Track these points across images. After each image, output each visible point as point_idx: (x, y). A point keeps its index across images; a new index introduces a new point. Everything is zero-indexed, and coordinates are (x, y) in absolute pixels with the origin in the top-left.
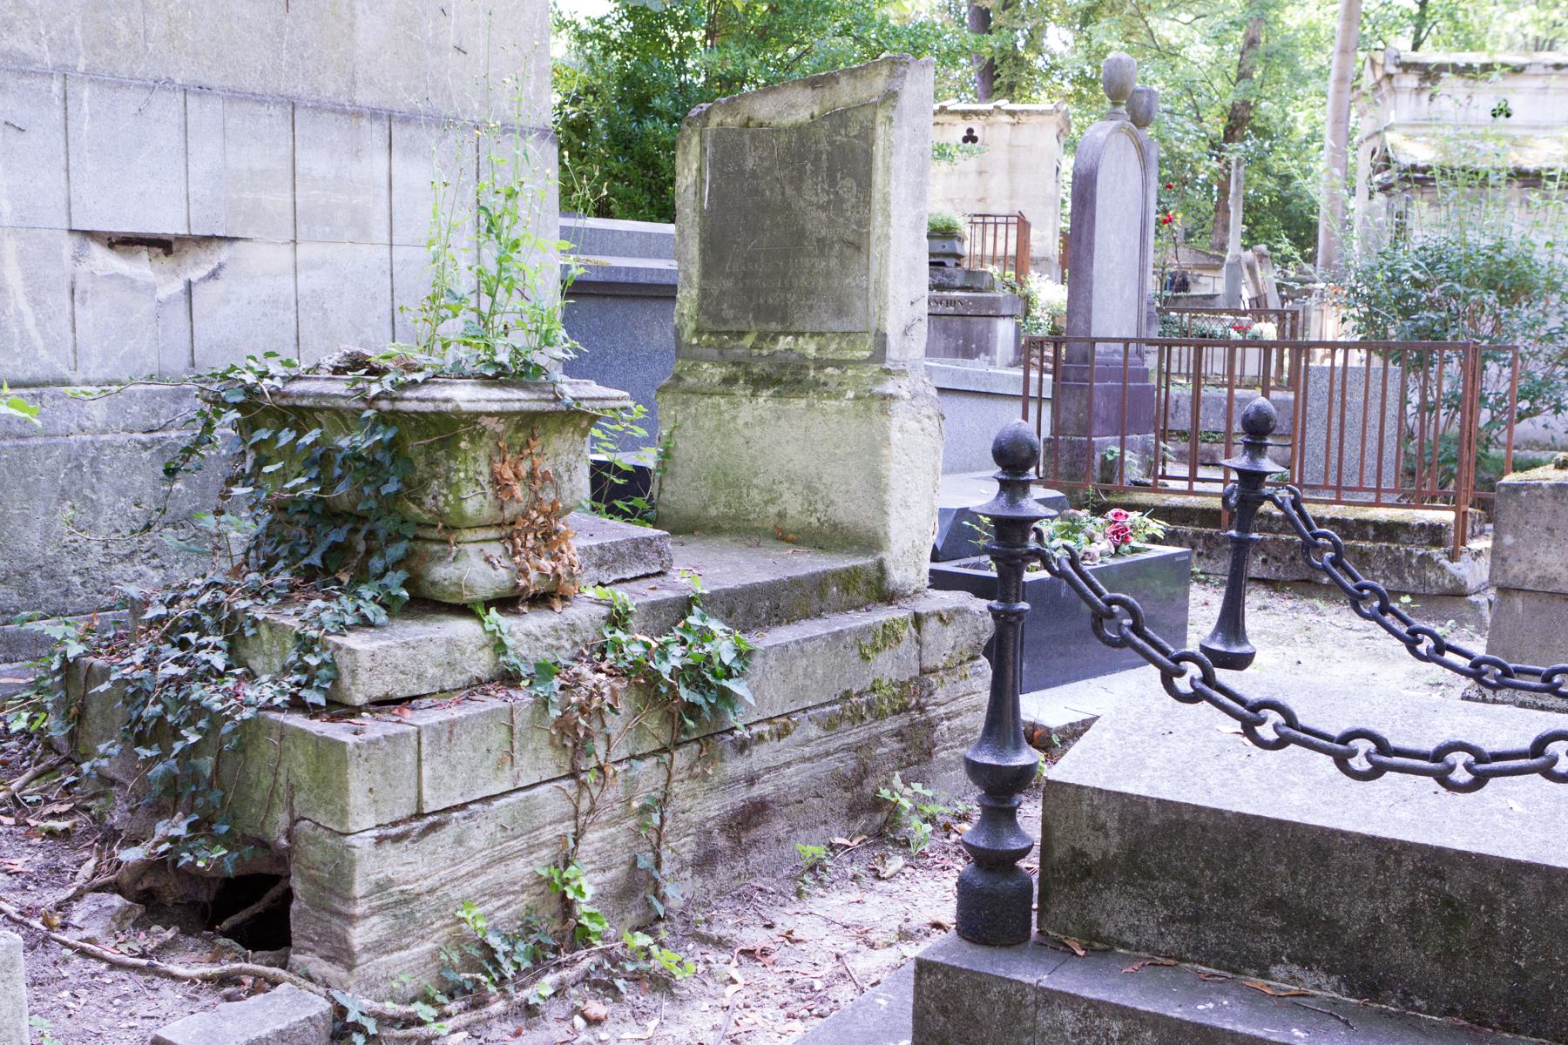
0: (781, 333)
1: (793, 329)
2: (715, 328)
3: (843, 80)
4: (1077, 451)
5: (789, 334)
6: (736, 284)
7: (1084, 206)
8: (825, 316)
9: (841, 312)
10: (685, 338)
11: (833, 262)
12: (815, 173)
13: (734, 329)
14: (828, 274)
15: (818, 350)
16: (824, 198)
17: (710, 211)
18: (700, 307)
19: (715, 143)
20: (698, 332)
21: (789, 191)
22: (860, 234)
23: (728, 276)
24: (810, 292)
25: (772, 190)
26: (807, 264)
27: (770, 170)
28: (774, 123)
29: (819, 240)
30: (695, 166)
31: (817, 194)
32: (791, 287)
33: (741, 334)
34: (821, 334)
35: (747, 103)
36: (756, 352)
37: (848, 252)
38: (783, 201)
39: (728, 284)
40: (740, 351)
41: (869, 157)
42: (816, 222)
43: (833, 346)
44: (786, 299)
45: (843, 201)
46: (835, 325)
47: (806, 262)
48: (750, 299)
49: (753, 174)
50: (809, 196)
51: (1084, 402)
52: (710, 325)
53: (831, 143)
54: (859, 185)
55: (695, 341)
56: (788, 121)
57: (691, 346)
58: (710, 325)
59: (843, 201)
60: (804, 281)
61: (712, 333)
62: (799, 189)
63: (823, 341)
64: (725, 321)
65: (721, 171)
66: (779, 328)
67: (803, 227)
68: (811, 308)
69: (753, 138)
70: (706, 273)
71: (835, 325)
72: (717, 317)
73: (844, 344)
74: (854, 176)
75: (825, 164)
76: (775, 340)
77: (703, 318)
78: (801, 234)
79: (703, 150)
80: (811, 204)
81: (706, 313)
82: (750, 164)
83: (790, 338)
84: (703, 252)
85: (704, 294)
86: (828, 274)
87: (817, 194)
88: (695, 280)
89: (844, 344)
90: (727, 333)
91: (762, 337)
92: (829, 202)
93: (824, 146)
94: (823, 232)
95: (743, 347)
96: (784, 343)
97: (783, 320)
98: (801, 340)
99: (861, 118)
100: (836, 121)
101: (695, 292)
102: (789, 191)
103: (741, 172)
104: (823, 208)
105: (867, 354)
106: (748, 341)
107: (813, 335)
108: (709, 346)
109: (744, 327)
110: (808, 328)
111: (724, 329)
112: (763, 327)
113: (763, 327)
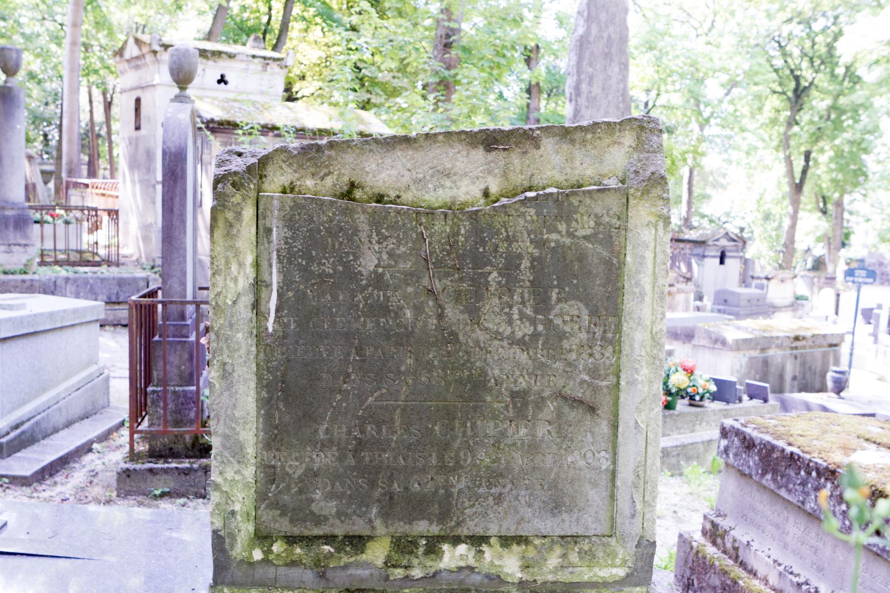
0: (442, 539)
1: (464, 531)
2: (296, 531)
3: (548, 144)
4: (182, 400)
5: (456, 541)
6: (341, 459)
7: (175, 181)
8: (527, 512)
9: (556, 505)
10: (238, 551)
11: (542, 430)
12: (509, 284)
13: (339, 531)
14: (533, 448)
15: (526, 567)
16: (524, 330)
17: (282, 338)
18: (261, 497)
19: (289, 222)
20: (262, 537)
21: (452, 313)
22: (596, 390)
23: (323, 446)
24: (495, 476)
25: (418, 309)
26: (491, 431)
27: (411, 277)
28: (407, 197)
29: (514, 395)
30: (250, 259)
31: (510, 322)
32: (458, 466)
33: (358, 542)
34: (521, 540)
35: (349, 157)
36: (399, 573)
37: (572, 415)
38: (440, 328)
39: (324, 459)
40: (365, 573)
41: (614, 271)
42: (507, 365)
43: (553, 561)
44: (447, 487)
45: (562, 336)
46: (550, 526)
47: (490, 428)
48: (373, 484)
49: (378, 280)
50: (493, 321)
51: (186, 356)
52: (285, 526)
53: (540, 244)
54: (594, 312)
55: (258, 555)
56: (437, 195)
57: (251, 564)
58: (285, 526)
59: (562, 336)
60: (484, 457)
61: (291, 540)
62: (474, 313)
63: (531, 553)
64: (319, 520)
65: (305, 270)
66: (435, 529)
67: (483, 373)
68: (499, 499)
69: (376, 222)
71: (550, 526)
72: (300, 512)
73: (574, 557)
74: (586, 299)
75: (526, 274)
76: (433, 548)
77: (267, 516)
78: (478, 385)
79: (263, 232)
80: (497, 336)
81: (275, 505)
82: (368, 263)
83: (462, 548)
84: (266, 404)
85: (270, 475)
86: (533, 448)
87: (510, 322)
88: (250, 451)
89: (574, 557)
90: (329, 539)
91: (404, 546)
92: (535, 336)
93: (525, 246)
94: (523, 384)
95: (368, 565)
96: (453, 556)
97: (443, 516)
98: (488, 553)
99: (598, 210)
100: (550, 209)
101: (249, 472)
102: (452, 313)
103: (351, 275)
104: (523, 344)
105: (621, 572)
106: (377, 553)
107: (506, 541)
108: (293, 564)
109: (359, 527)
110: (493, 530)
111: (317, 532)
112: (401, 528)
113: (401, 528)
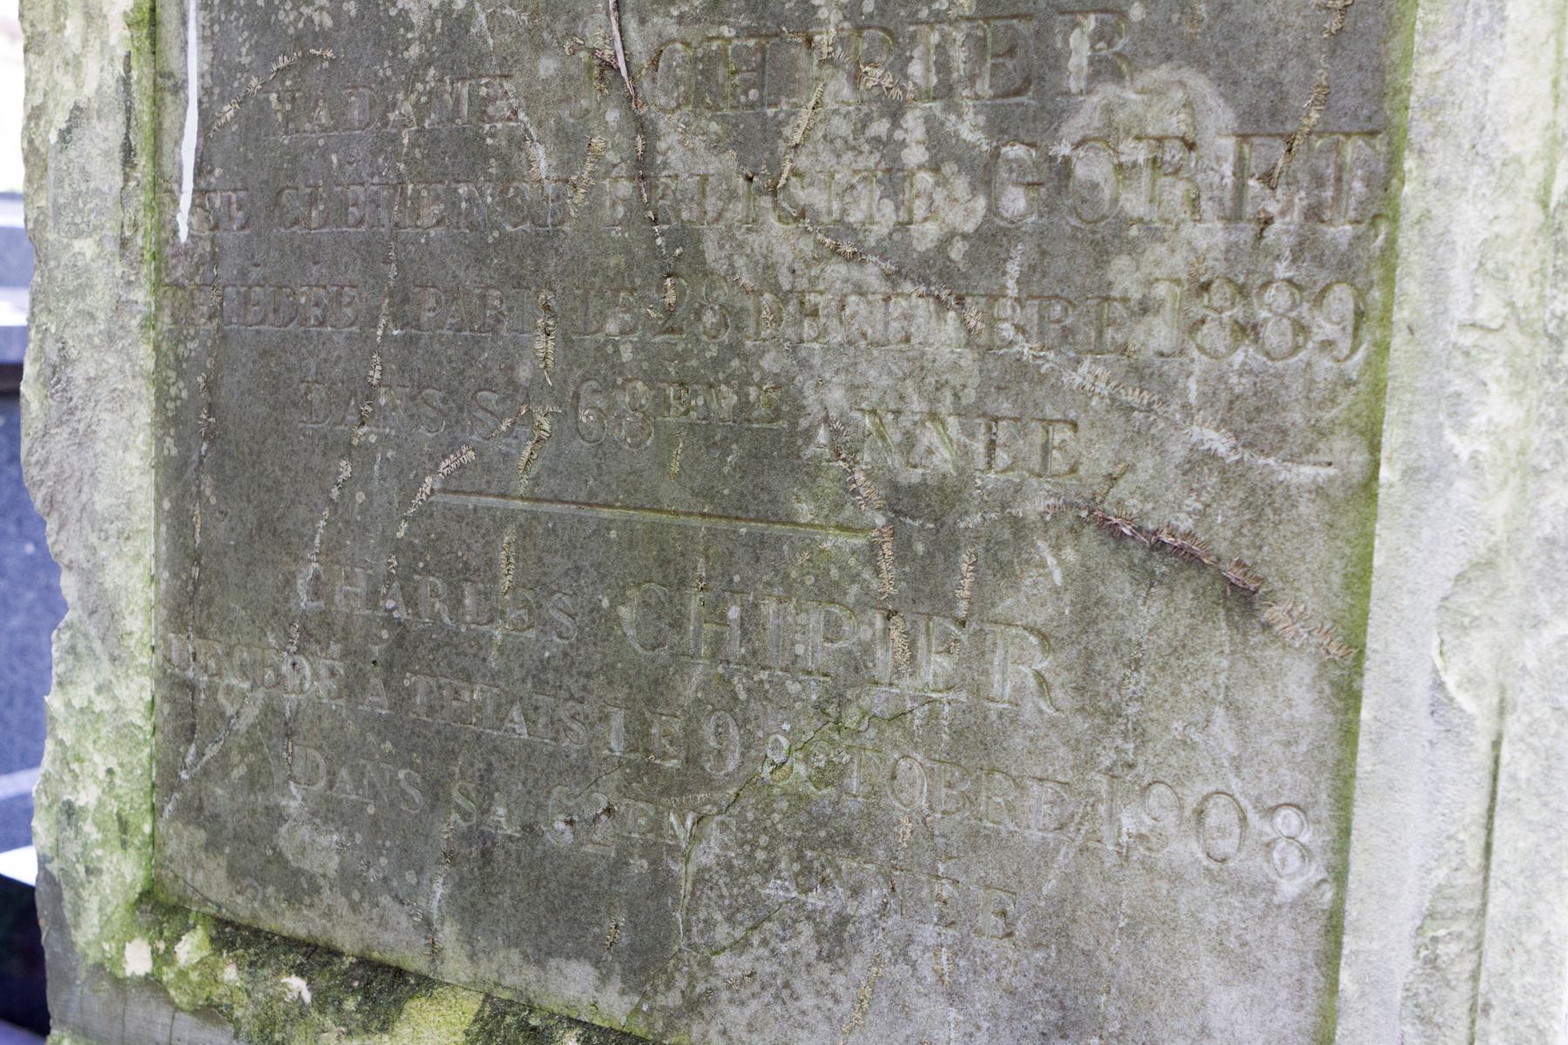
2: (243, 907)
6: (352, 687)
11: (1016, 671)
13: (347, 939)
16: (948, 212)
18: (166, 780)
20: (160, 908)
21: (686, 150)
22: (1262, 503)
23: (313, 633)
24: (827, 838)
25: (571, 142)
26: (813, 647)
29: (902, 502)
31: (894, 179)
32: (690, 779)
37: (1148, 614)
39: (310, 680)
42: (883, 371)
44: (658, 850)
45: (1108, 237)
47: (808, 634)
50: (830, 183)
52: (211, 882)
54: (1262, 119)
55: (138, 960)
59: (1108, 237)
60: (785, 753)
61: (230, 935)
64: (298, 887)
67: (787, 404)
68: (836, 939)
70: (191, 600)
72: (251, 847)
77: (184, 840)
78: (765, 449)
80: (843, 242)
81: (194, 811)
84: (175, 476)
85: (185, 711)
86: (974, 744)
87: (894, 179)
90: (313, 955)
92: (992, 239)
94: (941, 450)
101: (137, 692)
102: (686, 150)
104: (944, 278)
109: (398, 943)
111: (291, 924)
